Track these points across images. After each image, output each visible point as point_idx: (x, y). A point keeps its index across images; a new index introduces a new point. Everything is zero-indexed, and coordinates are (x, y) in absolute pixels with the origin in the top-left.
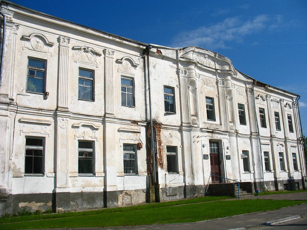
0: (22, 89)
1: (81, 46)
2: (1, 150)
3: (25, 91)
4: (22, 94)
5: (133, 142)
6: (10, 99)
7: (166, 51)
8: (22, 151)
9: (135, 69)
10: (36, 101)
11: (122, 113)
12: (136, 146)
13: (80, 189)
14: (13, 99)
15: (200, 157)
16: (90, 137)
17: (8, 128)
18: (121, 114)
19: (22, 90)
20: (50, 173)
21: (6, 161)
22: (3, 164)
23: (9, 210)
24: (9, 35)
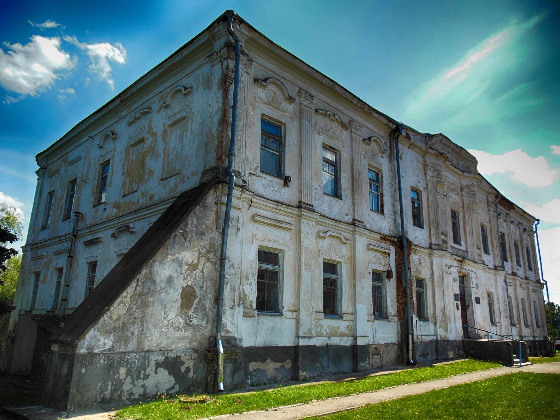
0: (255, 165)
2: (230, 268)
3: (258, 169)
4: (255, 173)
12: (384, 275)
13: (326, 340)
15: (452, 297)
20: (291, 311)
21: (237, 287)
22: (233, 292)
23: (238, 376)
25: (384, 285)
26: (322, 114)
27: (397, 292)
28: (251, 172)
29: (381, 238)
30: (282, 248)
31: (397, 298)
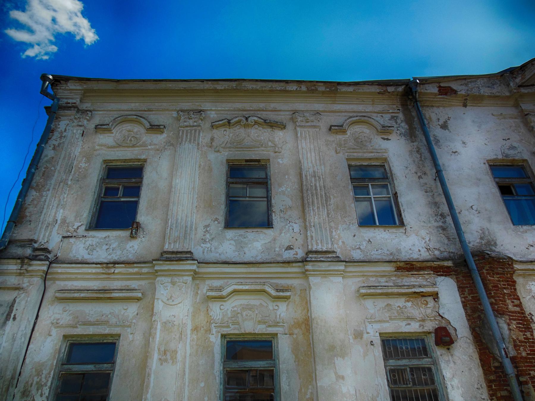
1: (229, 118)
3: (83, 227)
5: (414, 327)
6: (35, 250)
7: (466, 85)
8: (44, 380)
9: (384, 139)
10: (107, 247)
11: (361, 247)
12: (431, 341)
14: (47, 248)
16: (260, 322)
17: (14, 319)
18: (359, 248)
19: (75, 227)
24: (63, 130)
25: (435, 363)
26: (223, 125)
27: (485, 374)
28: (65, 235)
29: (398, 269)
30: (115, 331)
31: (489, 387)
